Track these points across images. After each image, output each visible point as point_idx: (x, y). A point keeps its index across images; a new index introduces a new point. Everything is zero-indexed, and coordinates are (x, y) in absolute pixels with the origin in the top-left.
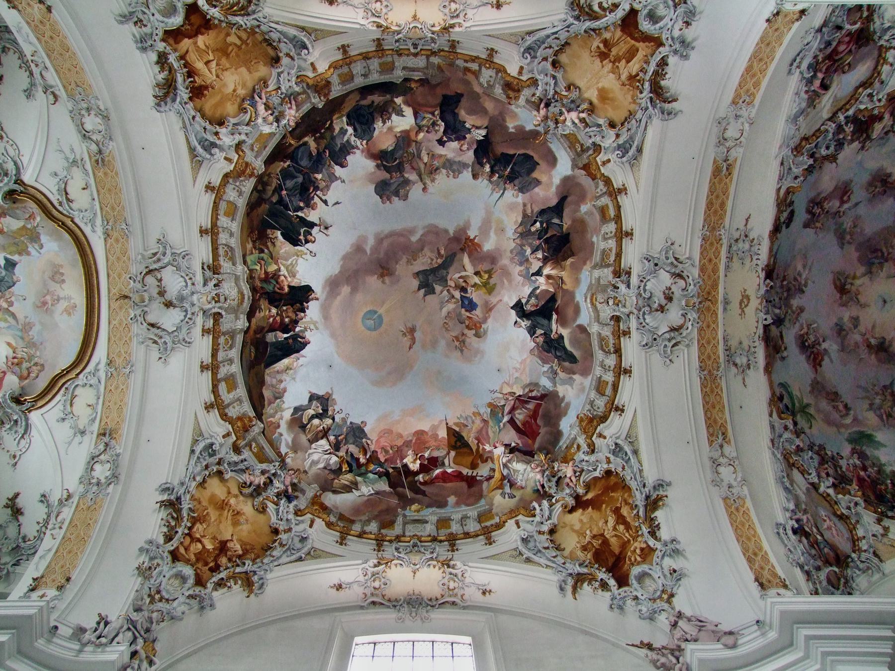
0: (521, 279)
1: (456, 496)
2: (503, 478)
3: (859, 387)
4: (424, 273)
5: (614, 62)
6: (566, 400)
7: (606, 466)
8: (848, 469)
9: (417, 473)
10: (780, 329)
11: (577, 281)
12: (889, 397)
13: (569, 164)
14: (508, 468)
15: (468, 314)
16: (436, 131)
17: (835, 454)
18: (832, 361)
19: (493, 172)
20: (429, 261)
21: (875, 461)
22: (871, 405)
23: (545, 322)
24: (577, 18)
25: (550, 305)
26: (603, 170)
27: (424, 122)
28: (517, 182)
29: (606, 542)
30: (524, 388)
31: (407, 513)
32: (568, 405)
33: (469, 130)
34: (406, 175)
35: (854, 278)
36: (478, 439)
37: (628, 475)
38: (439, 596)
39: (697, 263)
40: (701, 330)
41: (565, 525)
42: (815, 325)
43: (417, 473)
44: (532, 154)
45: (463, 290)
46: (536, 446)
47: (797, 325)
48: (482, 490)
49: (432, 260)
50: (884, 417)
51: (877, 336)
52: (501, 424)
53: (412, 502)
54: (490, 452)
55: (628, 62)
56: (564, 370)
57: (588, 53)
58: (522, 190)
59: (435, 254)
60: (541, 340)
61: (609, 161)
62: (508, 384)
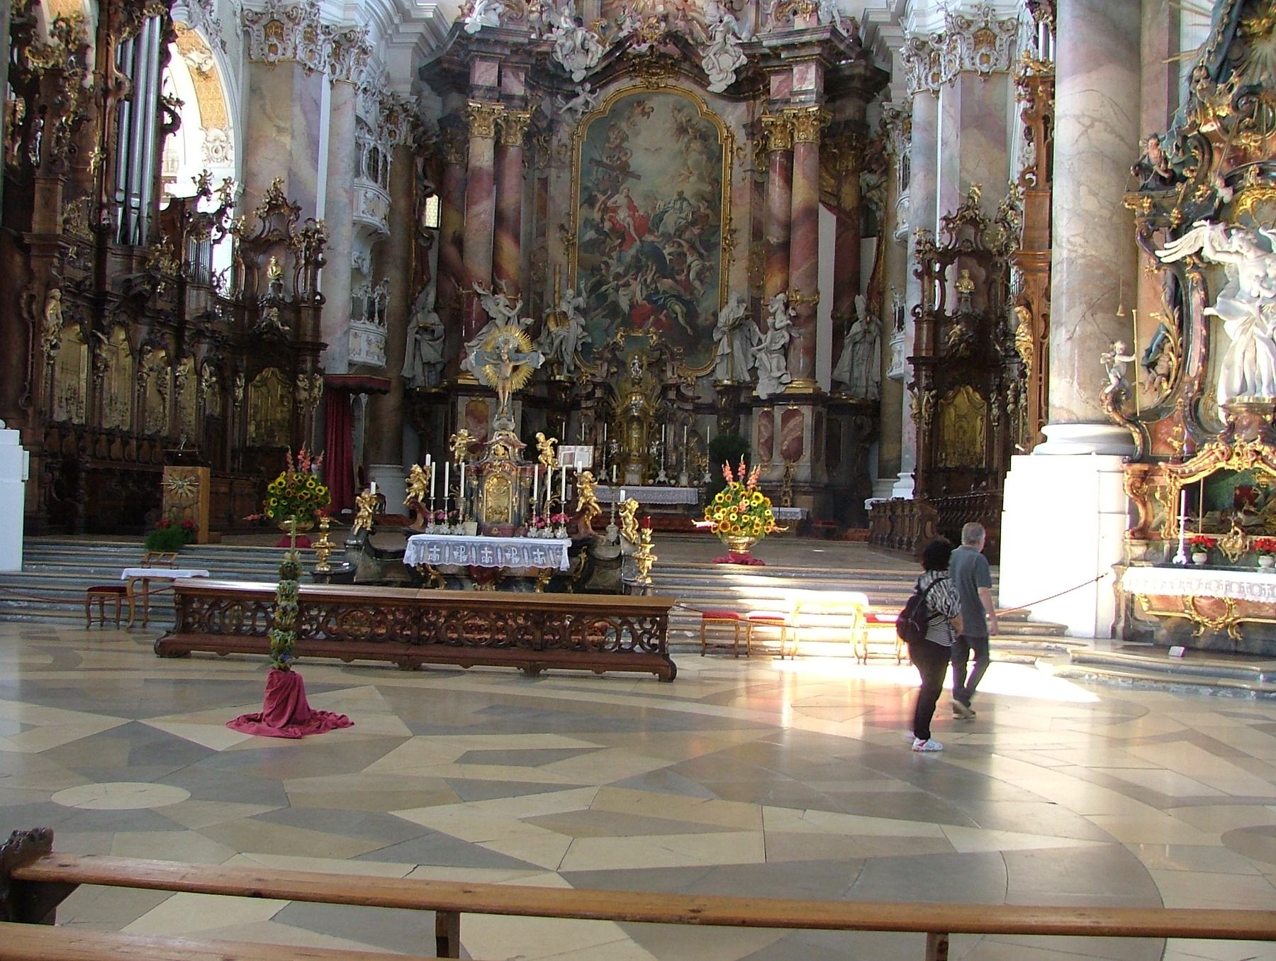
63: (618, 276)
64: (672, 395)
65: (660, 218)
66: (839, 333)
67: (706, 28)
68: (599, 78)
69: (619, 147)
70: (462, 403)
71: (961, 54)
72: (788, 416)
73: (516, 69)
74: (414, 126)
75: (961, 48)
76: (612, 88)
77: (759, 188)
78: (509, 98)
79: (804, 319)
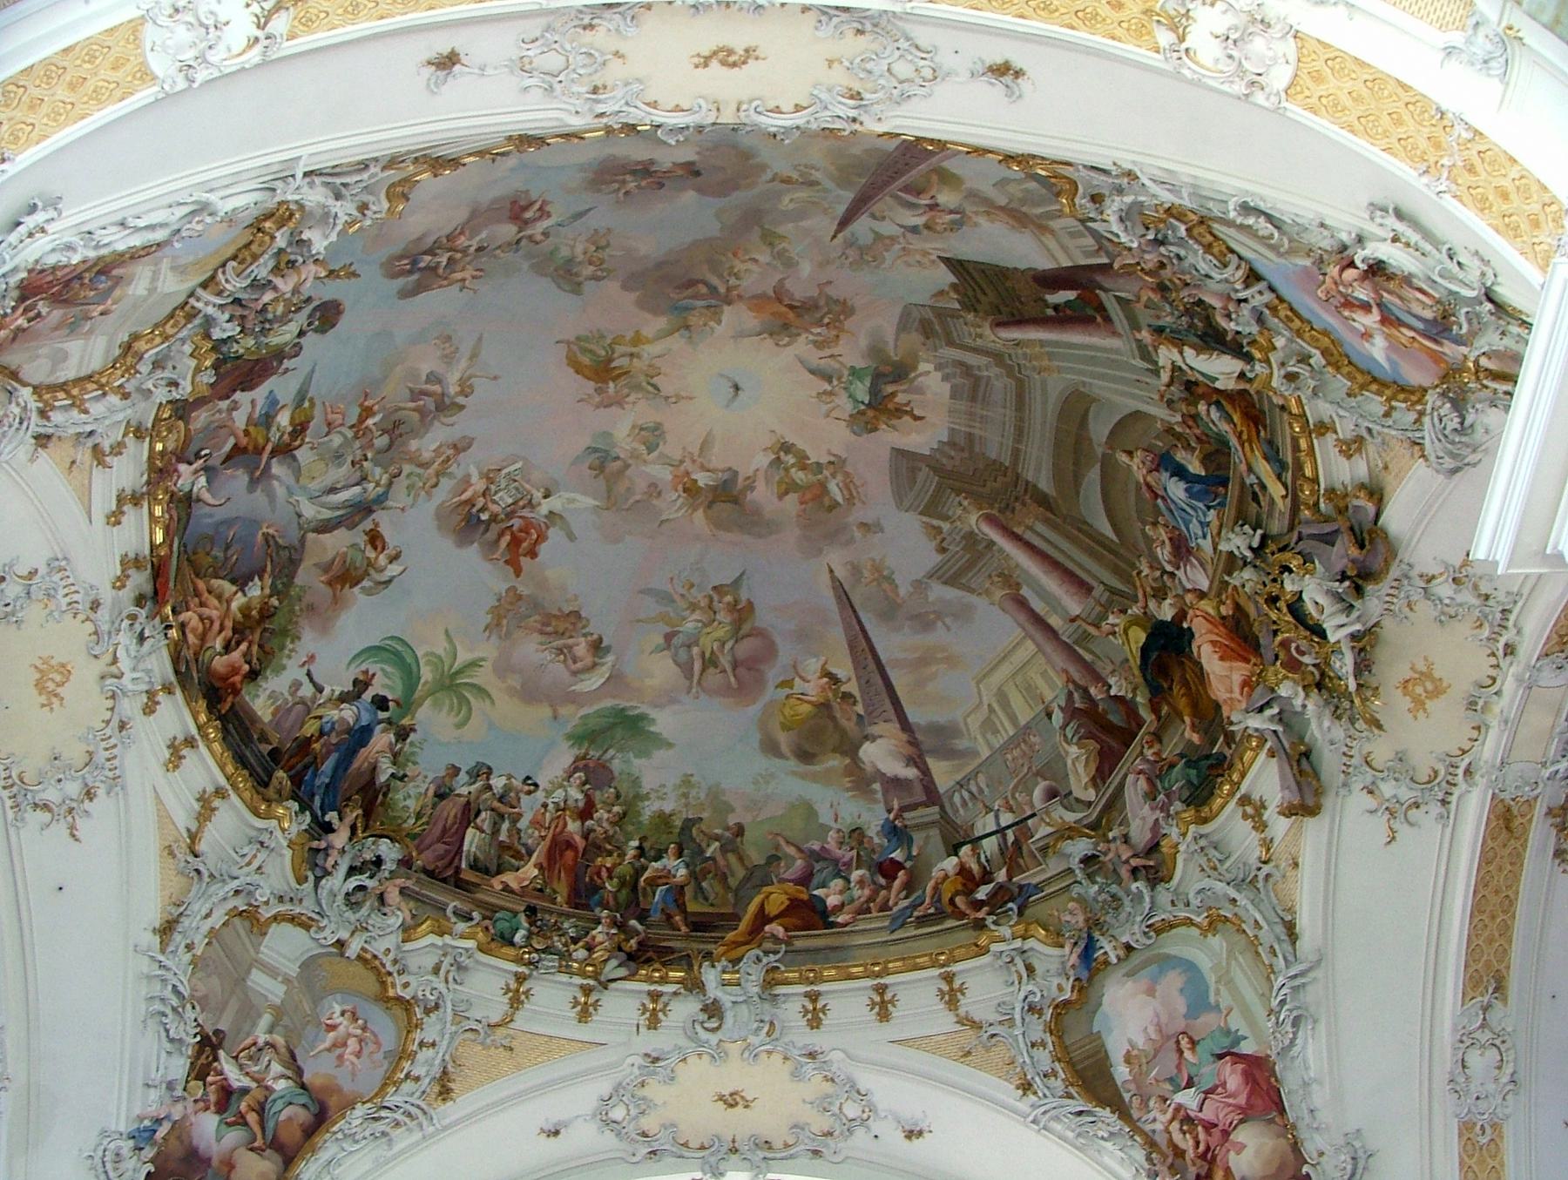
3: (647, 592)
8: (536, 824)
10: (367, 525)
12: (723, 616)
17: (517, 783)
18: (571, 537)
21: (624, 788)
22: (668, 637)
35: (637, 340)
42: (518, 465)
47: (446, 484)
50: (697, 666)
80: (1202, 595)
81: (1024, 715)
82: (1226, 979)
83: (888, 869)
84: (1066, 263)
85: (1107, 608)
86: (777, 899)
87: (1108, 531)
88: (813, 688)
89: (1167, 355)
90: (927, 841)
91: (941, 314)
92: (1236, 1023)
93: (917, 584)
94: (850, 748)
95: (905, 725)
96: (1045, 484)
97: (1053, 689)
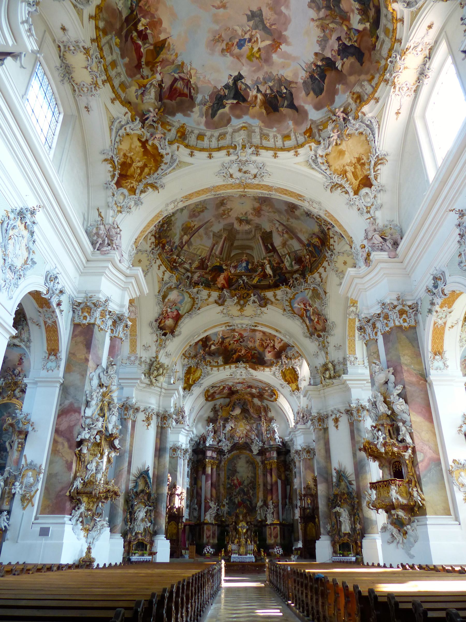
0: (255, 78)
1: (129, 62)
2: (145, 86)
4: (261, 15)
5: (354, 164)
6: (192, 114)
7: (164, 153)
9: (136, 30)
11: (253, 117)
13: (314, 119)
14: (150, 87)
15: (235, 43)
16: (346, 38)
19: (317, 66)
20: (268, 18)
23: (232, 96)
24: (378, 156)
25: (241, 98)
26: (307, 145)
27: (352, 34)
28: (309, 80)
29: (130, 165)
30: (195, 84)
31: (114, 38)
32: (189, 116)
33: (343, 60)
34: (323, 10)
36: (163, 60)
37: (163, 166)
38: (76, 82)
39: (260, 183)
40: (231, 184)
41: (132, 139)
43: (136, 30)
44: (324, 94)
45: (250, 40)
46: (166, 101)
48: (135, 75)
49: (269, 20)
51: (228, 202)
52: (173, 74)
53: (119, 36)
54: (157, 71)
55: (353, 173)
56: (207, 110)
57: (363, 152)
58: (305, 82)
59: (272, 22)
60: (222, 93)
61: (311, 150)
62: (196, 73)
63: (235, 495)
64: (249, 524)
65: (244, 482)
66: (283, 508)
67: (252, 440)
68: (230, 451)
69: (235, 466)
70: (205, 527)
71: (305, 455)
72: (274, 528)
73: (215, 451)
74: (192, 463)
75: (305, 454)
76: (233, 453)
77: (265, 475)
78: (213, 458)
79: (276, 506)
80: (230, 272)
81: (198, 253)
82: (186, 304)
83: (172, 251)
84: (277, 248)
85: (219, 258)
86: (163, 242)
87: (232, 255)
88: (192, 224)
89: (266, 262)
90: (176, 252)
91: (261, 229)
92: (182, 309)
93: (211, 231)
94: (185, 234)
95: (190, 239)
96: (235, 244)
97: (203, 255)
